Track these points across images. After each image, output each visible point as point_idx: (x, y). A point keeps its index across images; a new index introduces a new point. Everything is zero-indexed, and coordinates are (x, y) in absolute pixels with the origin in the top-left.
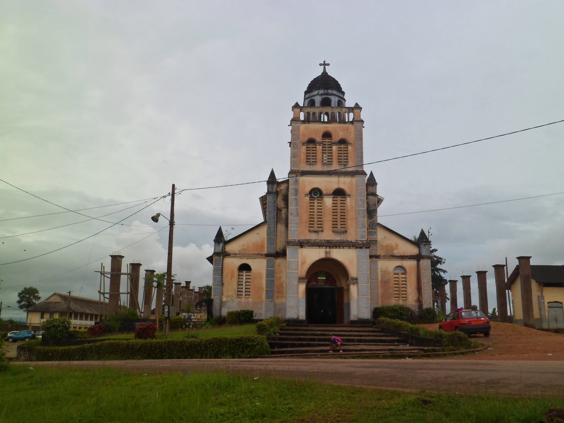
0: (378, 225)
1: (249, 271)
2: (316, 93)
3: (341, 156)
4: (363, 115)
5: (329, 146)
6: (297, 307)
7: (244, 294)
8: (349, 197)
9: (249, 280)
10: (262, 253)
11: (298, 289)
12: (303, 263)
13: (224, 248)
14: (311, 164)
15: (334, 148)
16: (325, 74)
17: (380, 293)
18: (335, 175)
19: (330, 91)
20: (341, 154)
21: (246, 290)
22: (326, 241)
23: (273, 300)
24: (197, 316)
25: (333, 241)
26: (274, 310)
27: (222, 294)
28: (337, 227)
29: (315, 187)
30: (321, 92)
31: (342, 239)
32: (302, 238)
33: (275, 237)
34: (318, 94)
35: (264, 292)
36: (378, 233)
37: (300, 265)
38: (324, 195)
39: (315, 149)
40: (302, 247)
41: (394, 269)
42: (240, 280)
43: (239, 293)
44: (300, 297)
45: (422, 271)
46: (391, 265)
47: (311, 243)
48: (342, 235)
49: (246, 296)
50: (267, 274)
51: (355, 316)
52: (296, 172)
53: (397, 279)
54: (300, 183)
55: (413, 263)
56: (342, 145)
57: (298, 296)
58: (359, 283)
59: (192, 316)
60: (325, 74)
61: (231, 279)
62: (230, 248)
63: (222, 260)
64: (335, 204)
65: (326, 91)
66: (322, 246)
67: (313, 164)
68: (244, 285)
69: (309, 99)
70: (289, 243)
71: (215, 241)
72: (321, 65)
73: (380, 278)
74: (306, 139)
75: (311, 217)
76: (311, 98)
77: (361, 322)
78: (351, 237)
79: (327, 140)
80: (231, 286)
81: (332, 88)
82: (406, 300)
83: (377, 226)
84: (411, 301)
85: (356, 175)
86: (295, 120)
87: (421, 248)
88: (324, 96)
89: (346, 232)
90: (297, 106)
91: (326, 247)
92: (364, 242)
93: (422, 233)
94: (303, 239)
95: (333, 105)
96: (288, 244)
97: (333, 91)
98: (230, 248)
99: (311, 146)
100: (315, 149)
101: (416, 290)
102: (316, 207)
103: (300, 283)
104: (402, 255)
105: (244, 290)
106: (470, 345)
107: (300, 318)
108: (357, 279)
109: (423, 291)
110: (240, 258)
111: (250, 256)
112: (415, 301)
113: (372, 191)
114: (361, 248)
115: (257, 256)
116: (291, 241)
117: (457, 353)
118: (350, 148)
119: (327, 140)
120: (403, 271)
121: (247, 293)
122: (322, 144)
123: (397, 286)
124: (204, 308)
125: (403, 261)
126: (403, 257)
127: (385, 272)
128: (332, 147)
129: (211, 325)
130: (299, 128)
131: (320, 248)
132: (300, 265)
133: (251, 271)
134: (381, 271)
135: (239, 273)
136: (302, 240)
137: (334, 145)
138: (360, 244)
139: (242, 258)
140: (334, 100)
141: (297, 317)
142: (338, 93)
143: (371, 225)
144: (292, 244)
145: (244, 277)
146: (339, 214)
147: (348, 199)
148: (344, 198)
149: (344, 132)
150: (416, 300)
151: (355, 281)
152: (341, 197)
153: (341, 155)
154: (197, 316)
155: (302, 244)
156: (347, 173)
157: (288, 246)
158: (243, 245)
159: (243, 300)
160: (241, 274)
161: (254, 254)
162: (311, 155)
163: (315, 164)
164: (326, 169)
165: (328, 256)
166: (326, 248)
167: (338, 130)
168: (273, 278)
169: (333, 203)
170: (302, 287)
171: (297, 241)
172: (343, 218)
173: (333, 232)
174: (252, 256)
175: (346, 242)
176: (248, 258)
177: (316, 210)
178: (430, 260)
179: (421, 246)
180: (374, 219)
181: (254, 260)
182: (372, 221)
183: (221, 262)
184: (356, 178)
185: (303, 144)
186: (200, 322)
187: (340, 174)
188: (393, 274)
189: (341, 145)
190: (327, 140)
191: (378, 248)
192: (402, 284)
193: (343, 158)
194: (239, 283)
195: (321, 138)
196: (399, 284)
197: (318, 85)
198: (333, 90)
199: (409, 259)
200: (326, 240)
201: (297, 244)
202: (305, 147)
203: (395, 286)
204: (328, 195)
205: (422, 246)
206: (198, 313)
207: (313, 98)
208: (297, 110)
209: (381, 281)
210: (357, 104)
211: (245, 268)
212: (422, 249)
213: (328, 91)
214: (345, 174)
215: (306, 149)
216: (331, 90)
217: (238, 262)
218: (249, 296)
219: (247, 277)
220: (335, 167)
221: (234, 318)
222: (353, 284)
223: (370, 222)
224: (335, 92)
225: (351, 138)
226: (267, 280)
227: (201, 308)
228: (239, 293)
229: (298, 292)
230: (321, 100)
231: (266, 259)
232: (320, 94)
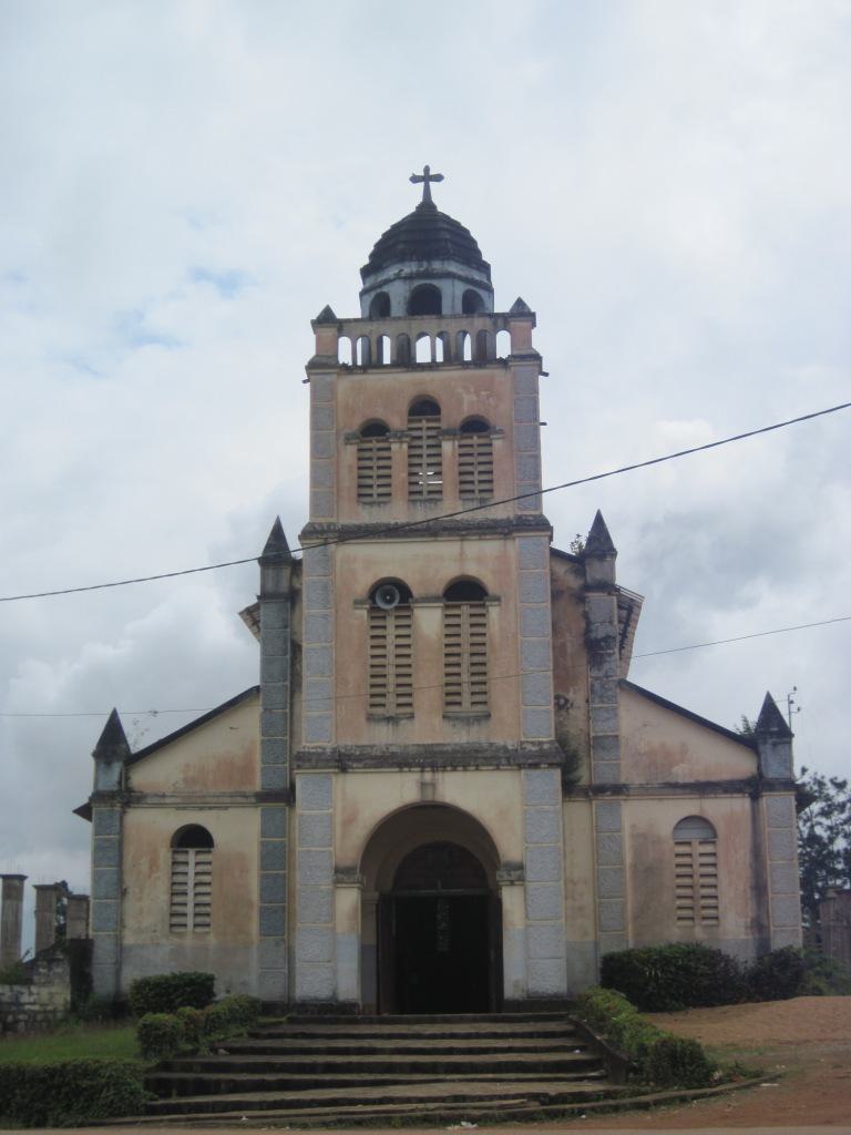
0: (621, 688)
1: (206, 849)
2: (391, 272)
3: (472, 473)
4: (540, 340)
5: (431, 442)
6: (329, 961)
7: (190, 921)
8: (497, 603)
9: (206, 879)
10: (248, 789)
11: (332, 903)
12: (349, 821)
13: (125, 778)
14: (371, 504)
15: (448, 447)
16: (427, 206)
17: (629, 906)
18: (450, 535)
19: (437, 265)
20: (472, 464)
21: (198, 910)
22: (422, 749)
23: (283, 940)
24: (38, 994)
25: (445, 749)
26: (286, 971)
27: (121, 924)
28: (460, 704)
29: (385, 574)
30: (410, 268)
31: (475, 740)
32: (347, 742)
33: (288, 738)
34: (398, 277)
35: (255, 916)
36: (622, 712)
37: (338, 829)
38: (417, 601)
39: (385, 454)
40: (344, 770)
41: (676, 828)
42: (179, 879)
43: (176, 920)
44: (339, 929)
45: (767, 829)
46: (665, 815)
47: (372, 758)
48: (475, 729)
49: (199, 930)
50: (263, 858)
51: (516, 985)
52: (323, 532)
53: (686, 860)
54: (338, 564)
55: (740, 805)
56: (475, 438)
57: (334, 929)
58: (528, 878)
59: (22, 994)
60: (427, 206)
61: (150, 877)
62: (142, 778)
63: (117, 816)
64: (451, 630)
65: (425, 264)
66: (409, 765)
67: (379, 504)
68: (191, 894)
69: (373, 294)
70: (303, 760)
71: (97, 755)
72: (415, 179)
73: (628, 859)
74: (357, 423)
75: (377, 674)
76: (379, 290)
77: (538, 1007)
78: (503, 732)
79: (424, 422)
80: (147, 904)
81: (445, 256)
82: (717, 926)
83: (618, 690)
84: (732, 933)
85: (519, 531)
86: (321, 365)
87: (763, 757)
88: (417, 283)
89: (488, 716)
90: (326, 320)
91: (423, 767)
92: (546, 747)
93: (770, 709)
94: (349, 743)
95: (446, 310)
96: (300, 763)
97: (446, 262)
98: (142, 778)
99: (374, 444)
100: (385, 454)
101: (749, 891)
102: (391, 641)
103: (339, 885)
104: (702, 778)
105: (190, 909)
106: (708, 1076)
107: (342, 997)
108: (521, 867)
109: (770, 895)
110: (178, 808)
111: (208, 800)
112: (747, 927)
113: (598, 577)
114: (535, 766)
115: (228, 800)
116: (309, 753)
117: (624, 1105)
118: (498, 444)
119: (424, 422)
120: (704, 834)
121: (200, 920)
122: (407, 436)
123: (687, 881)
124: (59, 970)
125: (703, 801)
126: (703, 788)
127: (644, 839)
128: (440, 446)
129: (82, 1022)
130: (332, 389)
131: (401, 772)
132: (338, 829)
133: (212, 849)
134: (633, 836)
135: (176, 856)
136: (346, 746)
137: (447, 437)
138: (532, 755)
139: (184, 808)
140: (452, 293)
141: (331, 994)
142: (465, 267)
143: (597, 686)
144: (314, 762)
145: (191, 869)
146: (466, 660)
147: (494, 612)
148: (481, 606)
149: (478, 396)
150: (749, 924)
151: (515, 874)
152: (472, 606)
153: (470, 468)
154: (38, 994)
155: (343, 762)
156: (489, 527)
157: (299, 767)
158: (187, 765)
159: (189, 941)
160: (181, 858)
161: (223, 795)
162: (374, 473)
163: (385, 503)
164: (421, 514)
165: (429, 797)
166: (422, 771)
167: (460, 390)
168: (284, 869)
169: (447, 626)
170: (349, 899)
171: (328, 751)
172: (480, 670)
173: (444, 717)
174: (215, 800)
175: (487, 750)
176: (201, 809)
177: (391, 650)
178: (793, 793)
179: (761, 748)
180: (606, 666)
181: (222, 813)
182: (601, 674)
183: (118, 823)
184: (517, 540)
185: (348, 440)
186: (50, 1012)
187: (466, 529)
188: (672, 842)
189: (472, 438)
190: (424, 424)
191: (623, 763)
192: (702, 876)
193: (476, 477)
194: (176, 887)
195: (406, 417)
196: (691, 876)
197: (401, 247)
198: (448, 259)
199: (726, 792)
200: (424, 745)
201: (328, 760)
202: (355, 448)
203: (679, 881)
204: (428, 599)
205: (766, 749)
206: (44, 985)
207: (385, 289)
208: (329, 332)
209: (635, 866)
210: (520, 302)
211: (193, 838)
212: (766, 760)
213: (430, 265)
214: (480, 531)
215: (355, 455)
216: (439, 259)
217: (173, 821)
218: (207, 929)
219: (200, 868)
220: (451, 506)
221: (153, 997)
222: (508, 883)
223: (597, 679)
224: (453, 267)
225: (500, 412)
226: (263, 878)
227: (50, 969)
228: (176, 920)
229: (332, 916)
230: (408, 295)
231: (260, 809)
232: (403, 274)
